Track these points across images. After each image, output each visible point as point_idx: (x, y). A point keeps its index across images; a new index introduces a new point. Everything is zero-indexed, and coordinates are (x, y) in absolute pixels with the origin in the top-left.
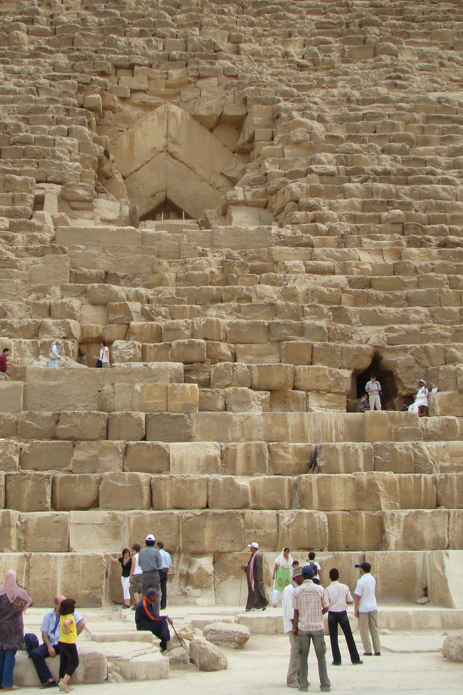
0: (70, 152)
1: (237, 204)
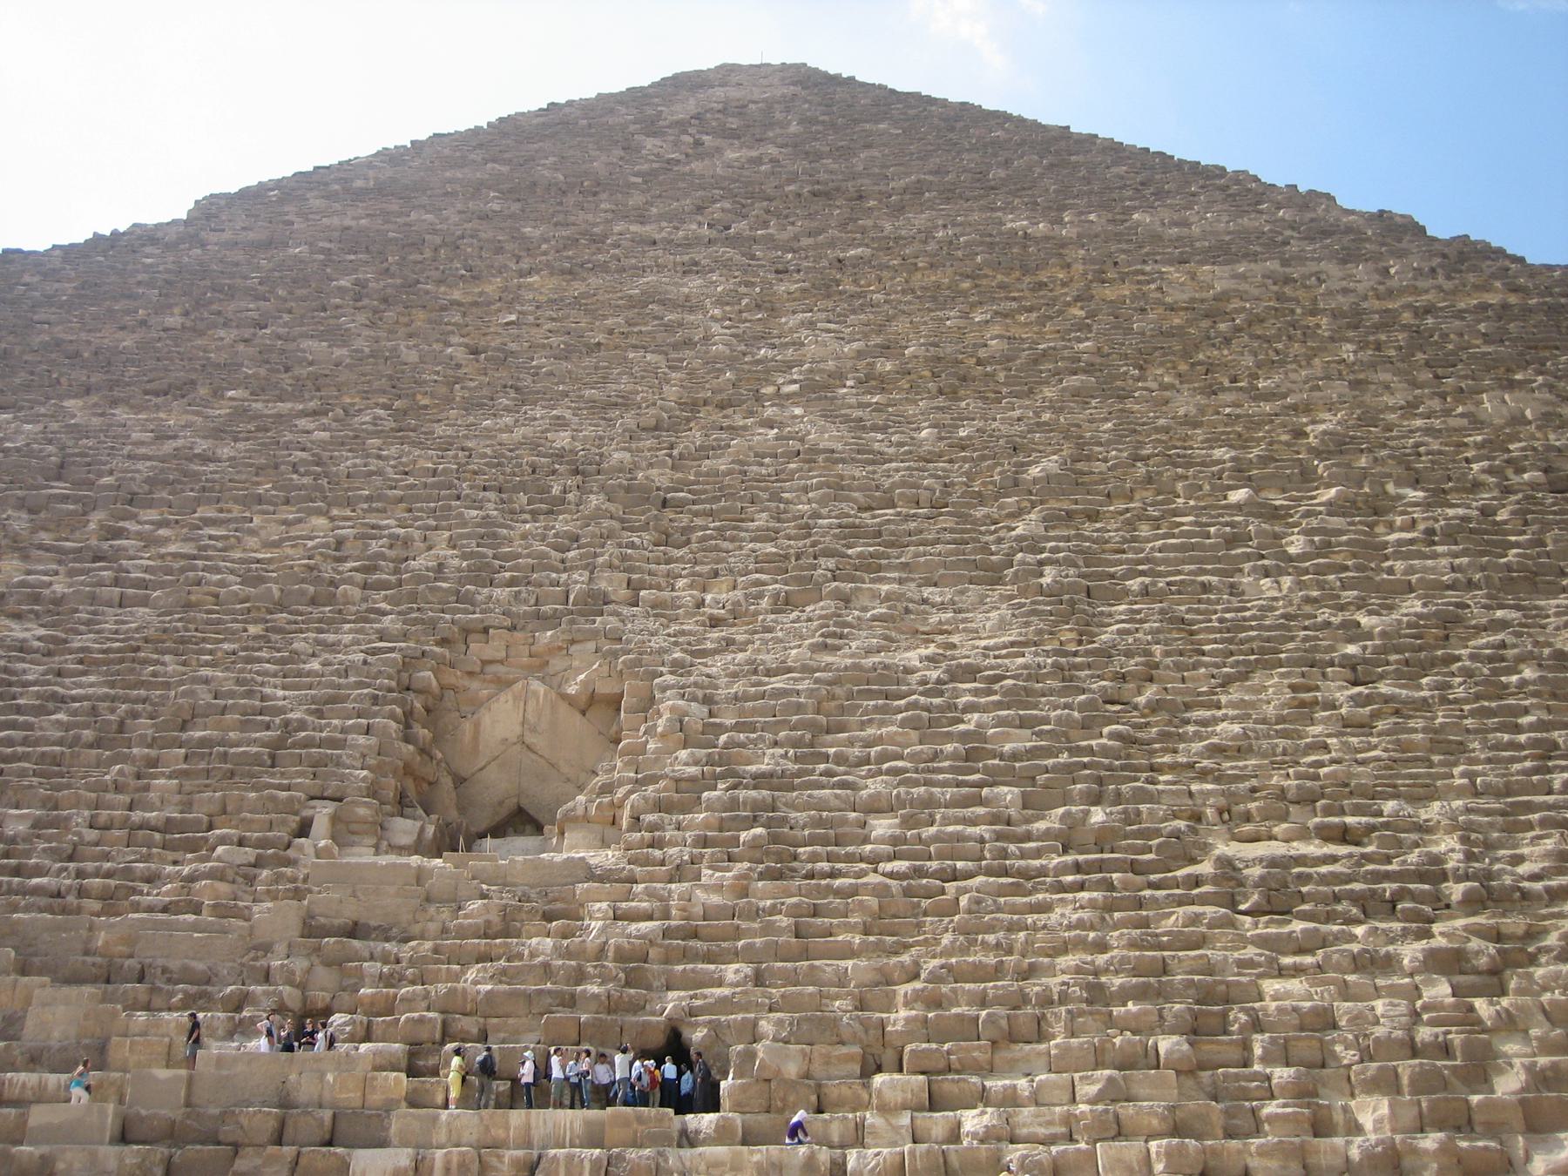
0: (364, 756)
1: (575, 820)
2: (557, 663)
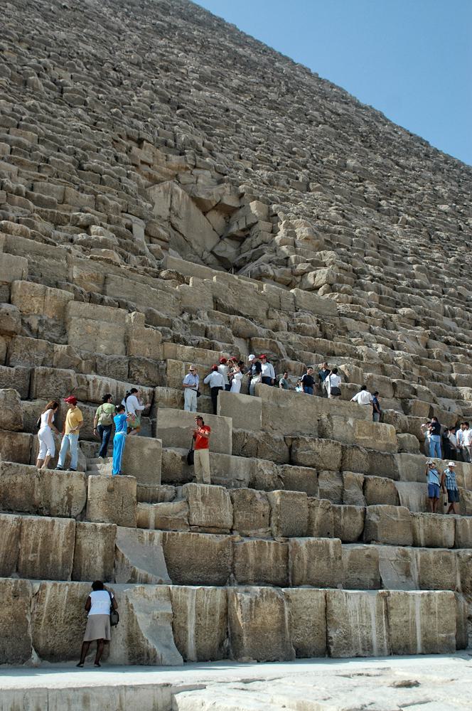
2: (185, 178)
